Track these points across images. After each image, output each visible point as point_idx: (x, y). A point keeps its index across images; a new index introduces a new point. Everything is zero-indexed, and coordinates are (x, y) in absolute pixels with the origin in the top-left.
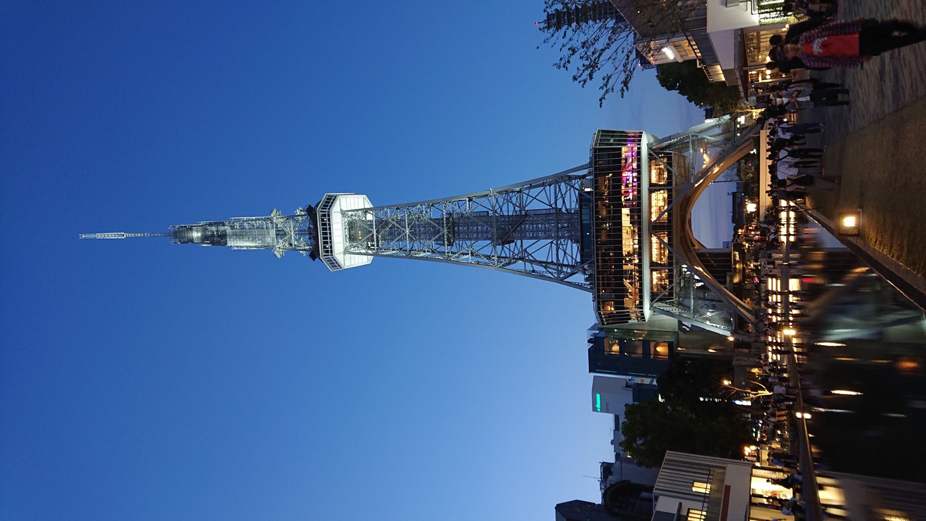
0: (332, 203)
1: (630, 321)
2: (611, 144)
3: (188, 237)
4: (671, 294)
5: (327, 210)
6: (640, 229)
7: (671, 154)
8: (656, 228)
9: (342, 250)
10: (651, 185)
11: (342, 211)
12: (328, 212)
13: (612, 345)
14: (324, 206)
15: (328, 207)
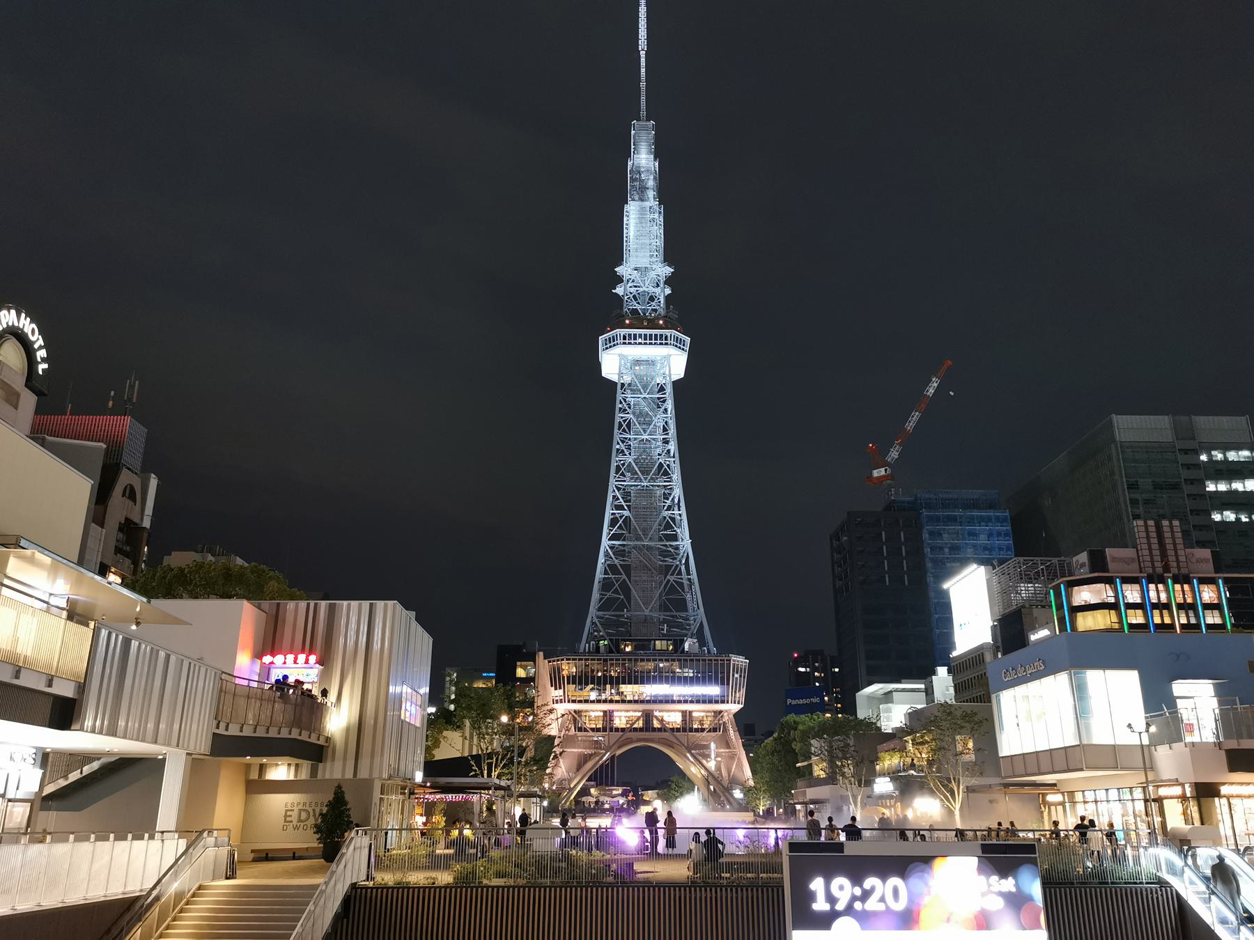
0: (680, 348)
1: (553, 688)
2: (733, 675)
3: (641, 145)
4: (580, 730)
5: (672, 342)
6: (648, 702)
7: (720, 731)
8: (648, 716)
9: (625, 353)
10: (690, 712)
11: (670, 356)
12: (671, 345)
13: (525, 668)
14: (677, 337)
15: (675, 343)
